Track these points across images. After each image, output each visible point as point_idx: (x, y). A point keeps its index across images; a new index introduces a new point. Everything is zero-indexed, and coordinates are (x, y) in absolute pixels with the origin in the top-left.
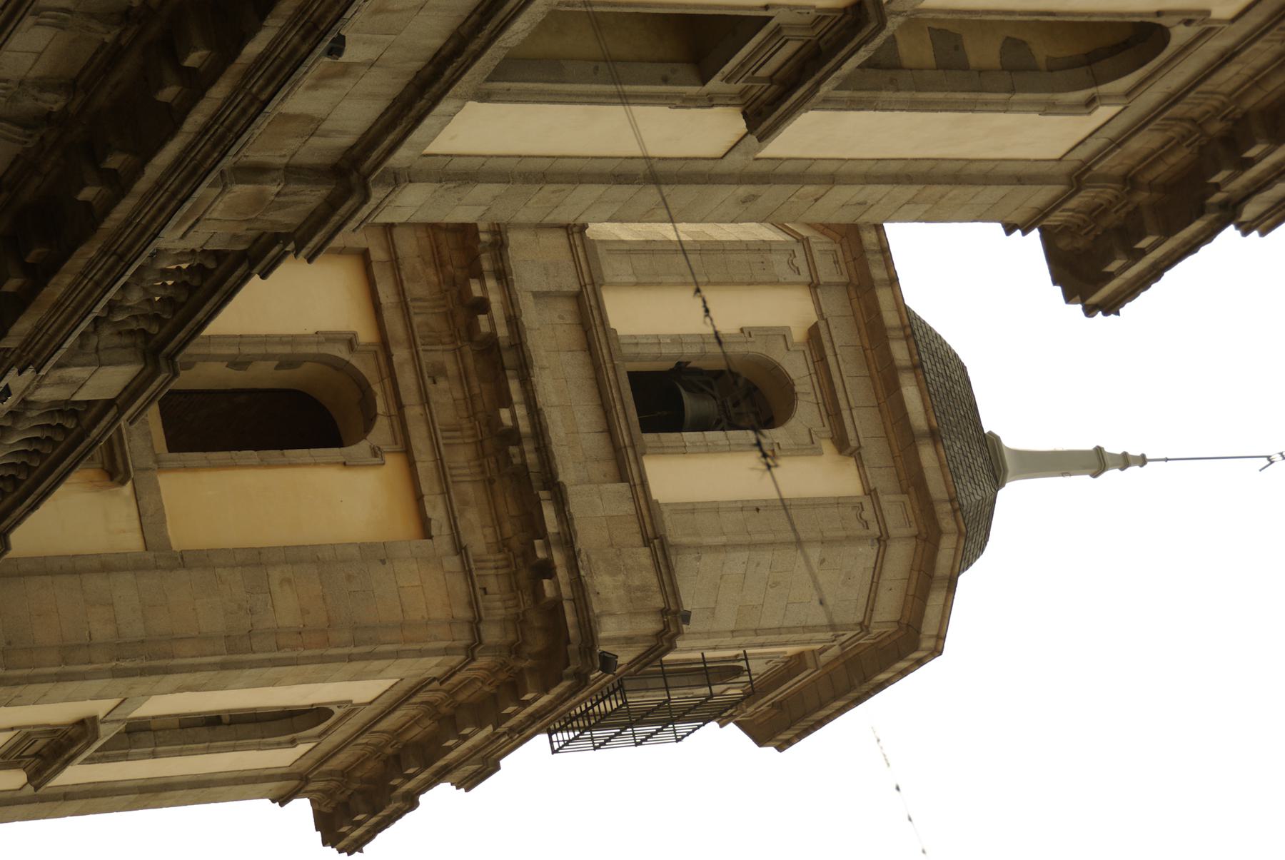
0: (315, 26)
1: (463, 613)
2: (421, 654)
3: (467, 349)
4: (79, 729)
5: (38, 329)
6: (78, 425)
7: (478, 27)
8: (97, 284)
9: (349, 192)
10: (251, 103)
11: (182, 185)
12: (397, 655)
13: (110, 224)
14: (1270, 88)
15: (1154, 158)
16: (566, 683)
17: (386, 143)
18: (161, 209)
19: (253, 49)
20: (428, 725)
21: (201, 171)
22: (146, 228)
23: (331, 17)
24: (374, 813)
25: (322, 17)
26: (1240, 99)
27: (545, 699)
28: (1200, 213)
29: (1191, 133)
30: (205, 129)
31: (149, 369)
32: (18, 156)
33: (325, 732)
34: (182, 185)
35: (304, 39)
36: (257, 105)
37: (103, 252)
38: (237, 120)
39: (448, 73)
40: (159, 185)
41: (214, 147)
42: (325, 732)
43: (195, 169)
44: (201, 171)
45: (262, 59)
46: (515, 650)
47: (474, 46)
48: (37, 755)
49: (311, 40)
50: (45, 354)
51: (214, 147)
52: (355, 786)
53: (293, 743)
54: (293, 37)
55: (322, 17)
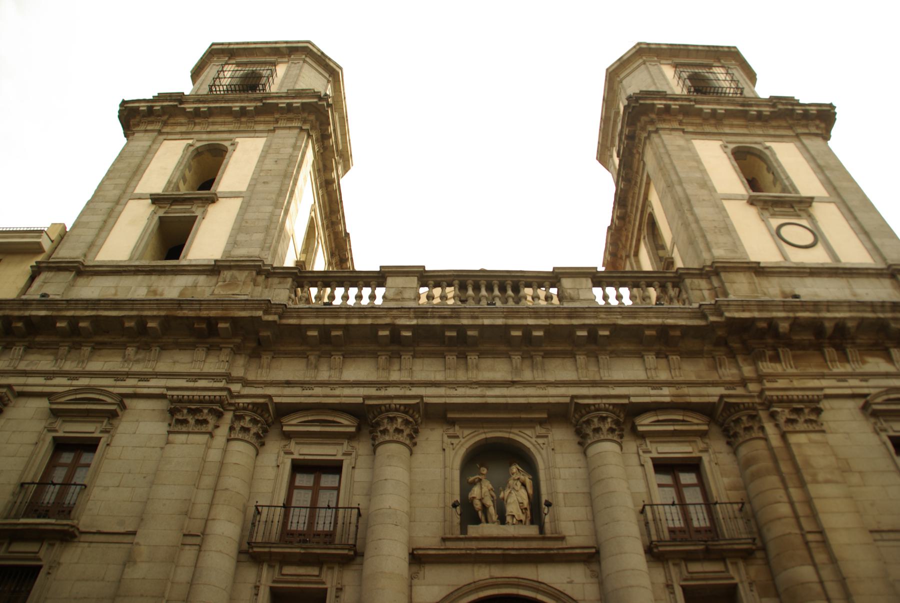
0: (23, 304)
1: (648, 142)
2: (663, 141)
3: (629, 210)
4: (755, 203)
5: (244, 310)
6: (454, 280)
7: (125, 271)
8: (201, 304)
9: (219, 266)
10: (70, 304)
11: (126, 304)
12: (665, 146)
13: (163, 313)
14: (223, 120)
15: (265, 122)
16: (641, 102)
17: (193, 268)
18: (150, 304)
19: (43, 313)
20: (726, 122)
21: (114, 302)
22: (156, 304)
23: (16, 302)
24: (793, 110)
25: (17, 304)
26: (232, 122)
27: (655, 102)
28: (264, 104)
29: (249, 122)
30: (93, 309)
31: (387, 275)
32: (180, 350)
33: (756, 143)
34: (126, 304)
35: (32, 304)
36: (70, 302)
37: (182, 309)
38: (81, 304)
39: (148, 269)
40: (132, 309)
41: (100, 304)
42: (756, 143)
43: (115, 304)
44: (114, 302)
45: (48, 310)
46: (652, 122)
47: (133, 269)
48: (792, 207)
49: (30, 302)
50: (257, 302)
51: (100, 304)
52: (791, 122)
53: (767, 148)
54: (34, 306)
55: (17, 304)
